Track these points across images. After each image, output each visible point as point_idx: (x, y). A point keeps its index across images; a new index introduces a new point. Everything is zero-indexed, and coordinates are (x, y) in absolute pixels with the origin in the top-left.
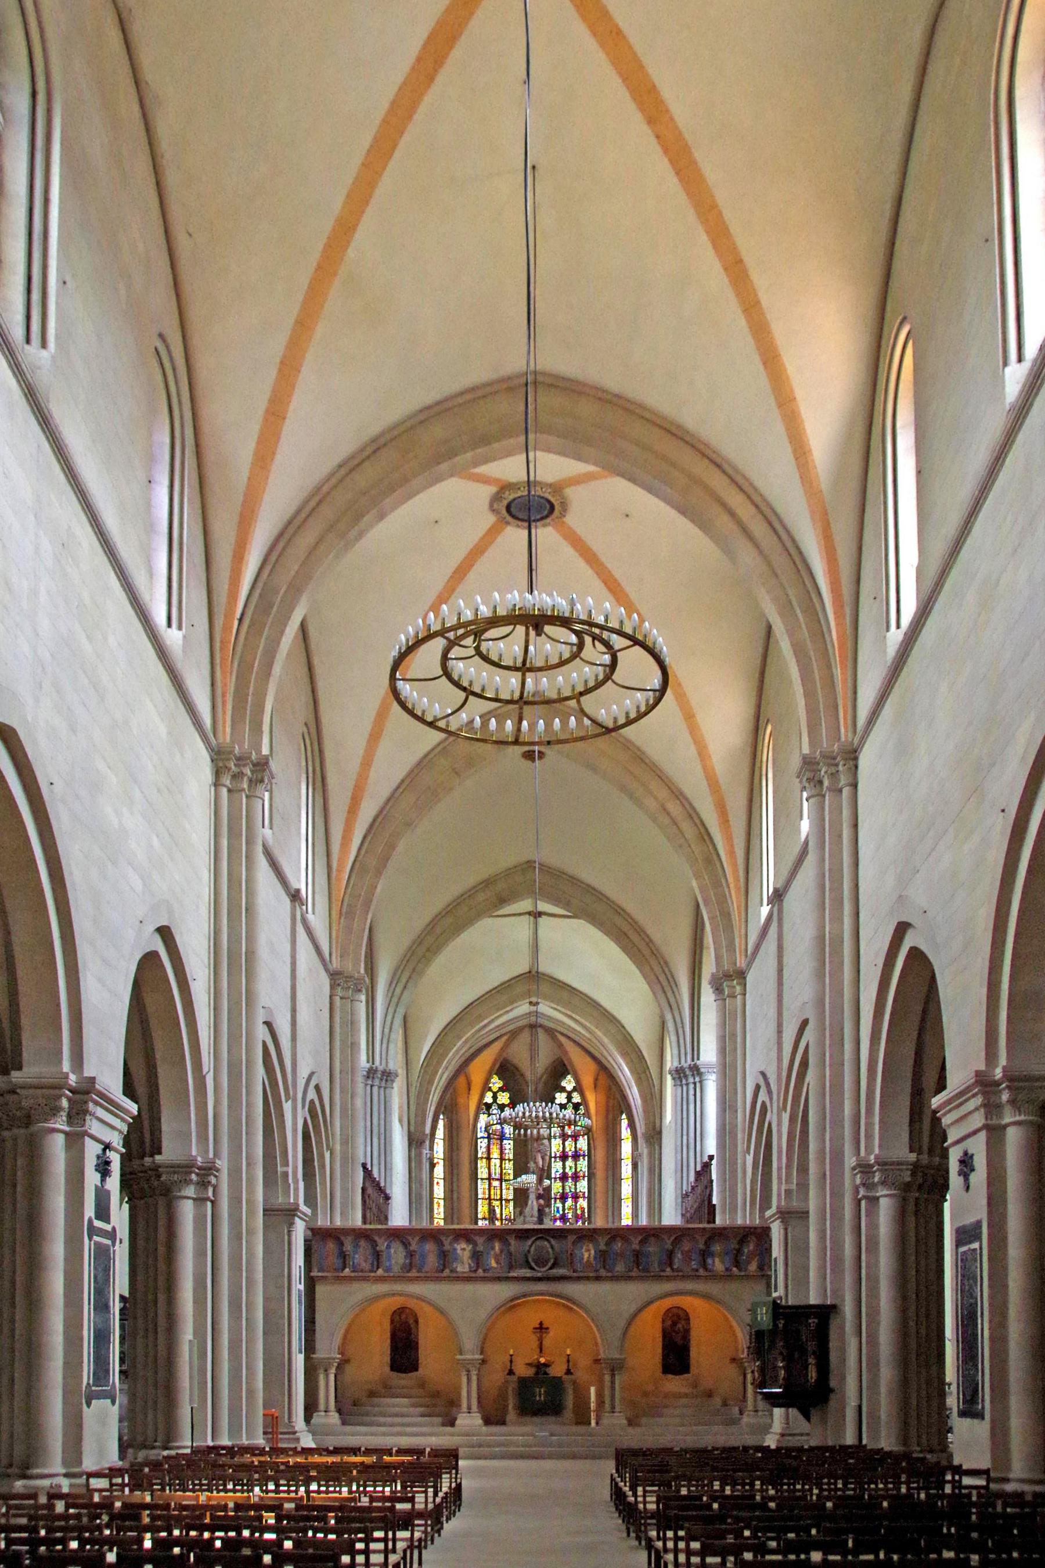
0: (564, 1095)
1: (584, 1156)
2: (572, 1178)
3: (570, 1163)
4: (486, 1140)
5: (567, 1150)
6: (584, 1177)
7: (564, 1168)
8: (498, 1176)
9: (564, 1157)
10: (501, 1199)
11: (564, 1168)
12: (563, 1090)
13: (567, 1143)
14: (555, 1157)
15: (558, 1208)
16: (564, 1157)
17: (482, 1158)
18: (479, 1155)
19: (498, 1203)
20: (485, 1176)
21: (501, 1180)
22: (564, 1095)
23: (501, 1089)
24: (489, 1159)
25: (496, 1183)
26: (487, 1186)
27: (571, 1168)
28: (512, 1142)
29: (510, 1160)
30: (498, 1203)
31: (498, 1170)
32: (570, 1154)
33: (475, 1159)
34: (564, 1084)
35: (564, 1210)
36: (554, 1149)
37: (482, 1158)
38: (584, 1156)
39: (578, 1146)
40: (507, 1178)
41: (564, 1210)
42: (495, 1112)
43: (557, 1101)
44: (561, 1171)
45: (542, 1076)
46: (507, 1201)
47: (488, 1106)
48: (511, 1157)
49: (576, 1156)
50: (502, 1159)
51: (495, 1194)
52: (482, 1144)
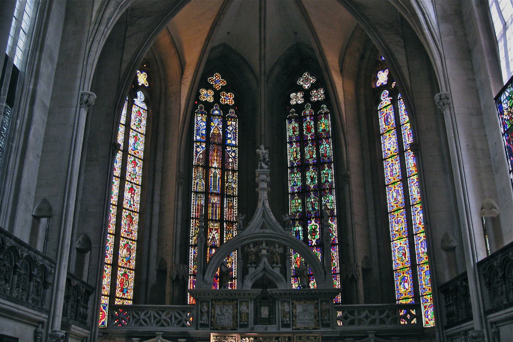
0: (300, 95)
1: (329, 163)
2: (315, 191)
3: (310, 173)
4: (204, 146)
5: (308, 157)
6: (331, 189)
7: (304, 179)
8: (218, 190)
9: (303, 167)
10: (221, 221)
11: (304, 179)
12: (300, 89)
13: (306, 149)
14: (292, 167)
15: (297, 232)
16: (303, 167)
17: (198, 166)
18: (195, 162)
19: (217, 225)
20: (201, 188)
21: (222, 195)
22: (300, 95)
23: (223, 88)
24: (207, 167)
25: (215, 200)
26: (203, 202)
27: (312, 179)
28: (237, 150)
29: (233, 171)
30: (217, 225)
31: (218, 183)
32: (311, 161)
33: (189, 166)
34: (300, 82)
35: (305, 234)
36: (290, 158)
37: (198, 166)
38: (329, 163)
39: (322, 151)
40: (230, 193)
41: (305, 234)
42: (216, 112)
43: (293, 102)
44: (299, 184)
45: (272, 70)
46: (231, 223)
47: (208, 106)
48: (236, 167)
49: (319, 165)
50: (224, 169)
51: (214, 213)
52: (200, 149)
